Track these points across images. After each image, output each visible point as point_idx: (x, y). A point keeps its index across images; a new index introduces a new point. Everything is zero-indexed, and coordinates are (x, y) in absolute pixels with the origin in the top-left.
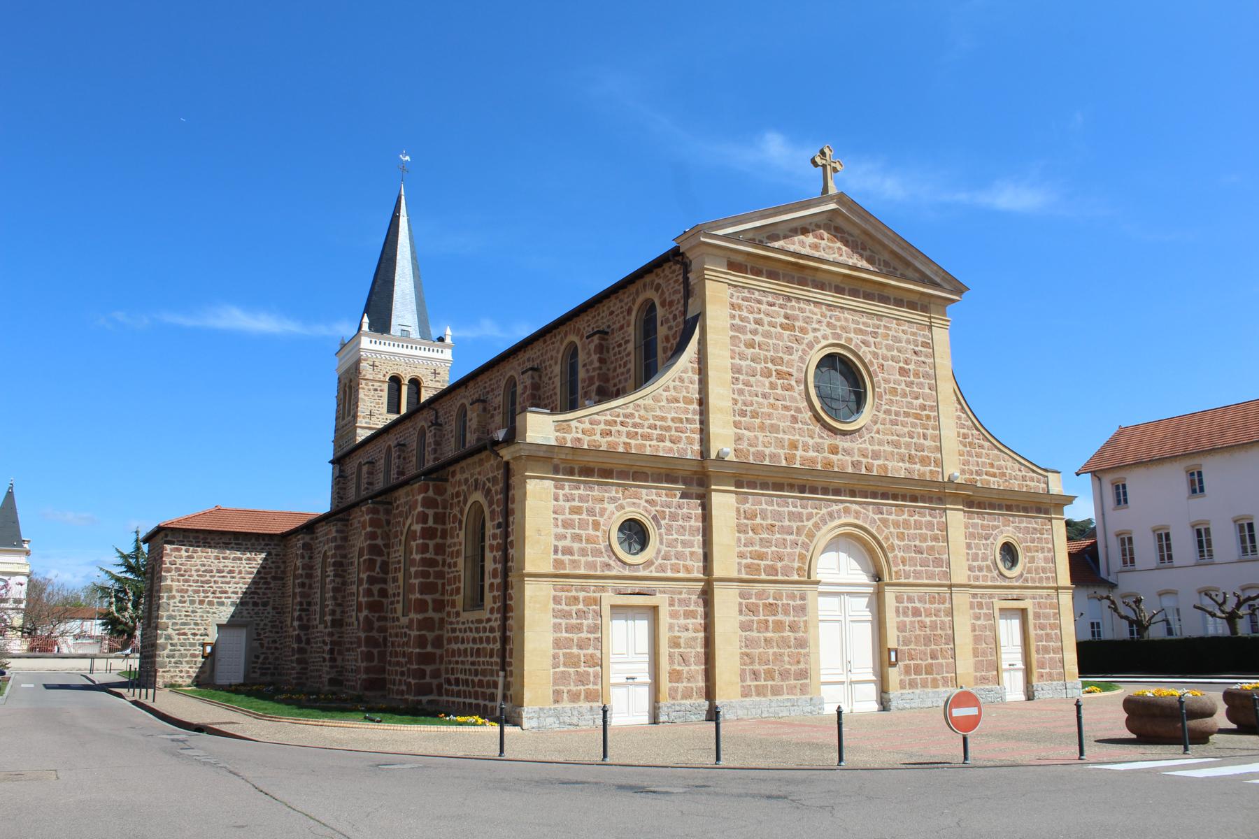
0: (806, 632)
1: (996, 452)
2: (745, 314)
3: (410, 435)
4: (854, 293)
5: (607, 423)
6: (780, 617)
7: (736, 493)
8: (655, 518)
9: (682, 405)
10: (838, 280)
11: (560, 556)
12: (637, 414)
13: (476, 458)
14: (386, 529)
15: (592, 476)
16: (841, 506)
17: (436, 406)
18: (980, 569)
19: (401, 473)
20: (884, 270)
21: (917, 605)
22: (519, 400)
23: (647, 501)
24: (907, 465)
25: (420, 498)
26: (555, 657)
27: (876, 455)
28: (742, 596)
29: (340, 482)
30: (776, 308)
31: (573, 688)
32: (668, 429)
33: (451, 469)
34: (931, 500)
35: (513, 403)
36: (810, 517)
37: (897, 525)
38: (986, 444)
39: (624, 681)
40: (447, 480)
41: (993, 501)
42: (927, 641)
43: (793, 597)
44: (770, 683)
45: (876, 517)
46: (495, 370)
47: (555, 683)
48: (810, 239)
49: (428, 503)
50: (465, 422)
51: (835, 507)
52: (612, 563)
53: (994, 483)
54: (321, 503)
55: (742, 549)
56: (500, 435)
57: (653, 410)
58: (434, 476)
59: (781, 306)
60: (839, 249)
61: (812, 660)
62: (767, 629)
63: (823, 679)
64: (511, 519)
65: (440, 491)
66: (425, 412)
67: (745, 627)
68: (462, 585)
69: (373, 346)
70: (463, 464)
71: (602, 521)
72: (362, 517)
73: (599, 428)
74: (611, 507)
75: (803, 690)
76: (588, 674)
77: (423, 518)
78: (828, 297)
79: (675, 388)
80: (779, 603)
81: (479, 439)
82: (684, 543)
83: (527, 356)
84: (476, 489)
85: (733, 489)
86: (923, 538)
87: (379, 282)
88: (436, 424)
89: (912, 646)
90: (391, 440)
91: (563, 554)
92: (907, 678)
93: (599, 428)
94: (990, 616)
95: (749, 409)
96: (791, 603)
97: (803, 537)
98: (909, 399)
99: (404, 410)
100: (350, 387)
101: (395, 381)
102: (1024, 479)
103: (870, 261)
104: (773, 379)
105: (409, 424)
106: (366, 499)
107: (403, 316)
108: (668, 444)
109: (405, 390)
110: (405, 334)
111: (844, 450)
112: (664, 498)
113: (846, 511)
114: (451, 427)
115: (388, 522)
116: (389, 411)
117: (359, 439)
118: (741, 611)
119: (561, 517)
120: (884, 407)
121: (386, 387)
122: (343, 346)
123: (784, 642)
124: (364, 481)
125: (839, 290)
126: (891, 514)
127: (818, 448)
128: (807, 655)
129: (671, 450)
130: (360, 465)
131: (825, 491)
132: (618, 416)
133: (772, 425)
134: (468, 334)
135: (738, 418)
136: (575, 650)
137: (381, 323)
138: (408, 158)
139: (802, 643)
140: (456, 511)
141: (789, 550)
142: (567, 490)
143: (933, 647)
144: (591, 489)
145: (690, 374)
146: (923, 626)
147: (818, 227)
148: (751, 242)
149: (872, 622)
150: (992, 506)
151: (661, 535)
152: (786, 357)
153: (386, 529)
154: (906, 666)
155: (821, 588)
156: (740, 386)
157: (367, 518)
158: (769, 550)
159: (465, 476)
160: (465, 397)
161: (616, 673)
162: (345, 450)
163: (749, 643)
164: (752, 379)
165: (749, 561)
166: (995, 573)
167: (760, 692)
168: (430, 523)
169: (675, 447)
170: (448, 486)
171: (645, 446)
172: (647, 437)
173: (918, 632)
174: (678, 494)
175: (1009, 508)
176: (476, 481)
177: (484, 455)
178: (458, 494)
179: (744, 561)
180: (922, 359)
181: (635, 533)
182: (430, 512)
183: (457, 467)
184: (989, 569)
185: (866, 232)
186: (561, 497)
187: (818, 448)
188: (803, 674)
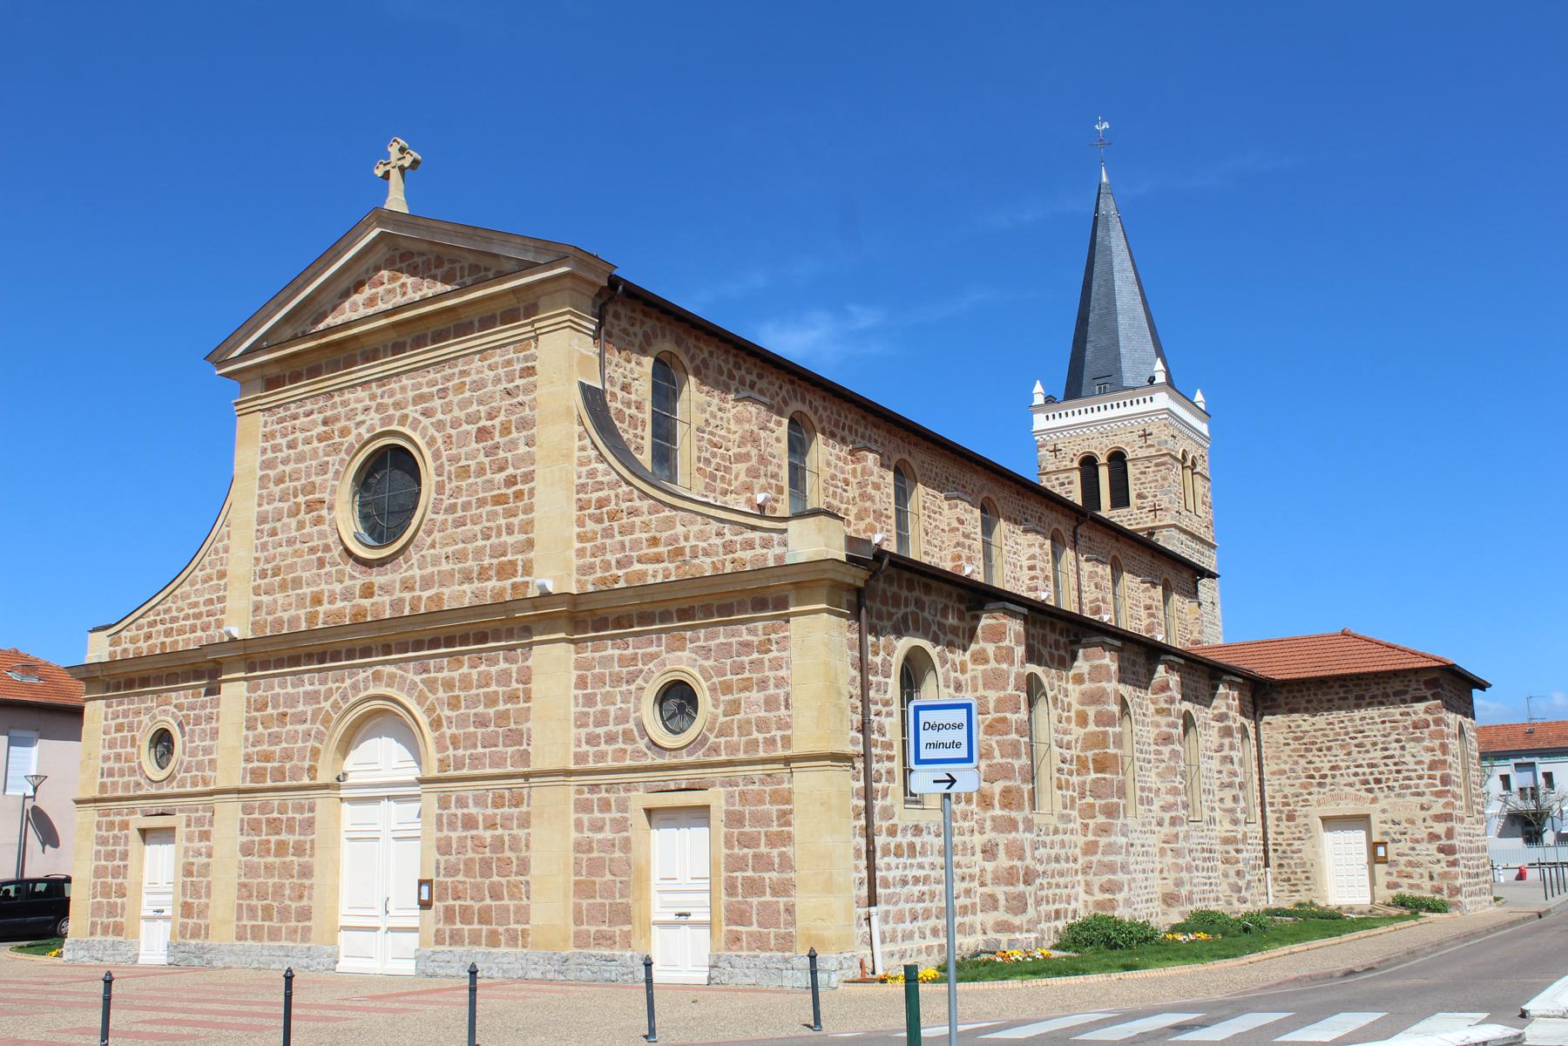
0: (312, 856)
1: (667, 513)
4: (419, 342)
6: (284, 836)
7: (245, 679)
8: (180, 725)
10: (392, 335)
16: (370, 671)
18: (611, 738)
20: (468, 280)
21: (472, 810)
24: (476, 584)
27: (427, 583)
34: (510, 634)
36: (329, 693)
38: (645, 505)
39: (673, 918)
41: (647, 608)
42: (486, 866)
43: (299, 808)
44: (267, 923)
45: (418, 679)
48: (367, 292)
51: (362, 675)
52: (142, 781)
53: (654, 573)
55: (251, 750)
60: (403, 285)
62: (268, 852)
63: (343, 922)
67: (246, 850)
69: (1052, 424)
75: (306, 934)
85: (242, 674)
86: (491, 700)
89: (460, 878)
92: (447, 928)
94: (621, 825)
96: (298, 816)
97: (318, 725)
102: (729, 548)
103: (445, 281)
109: (1104, 474)
111: (381, 588)
112: (191, 699)
113: (377, 677)
120: (447, 502)
123: (286, 870)
125: (398, 348)
126: (440, 669)
128: (311, 887)
131: (351, 654)
138: (1106, 125)
139: (306, 872)
143: (495, 878)
146: (479, 845)
147: (378, 269)
148: (270, 349)
150: (646, 618)
152: (318, 480)
154: (447, 908)
161: (660, 907)
163: (250, 870)
165: (256, 764)
166: (642, 744)
167: (257, 934)
172: (181, 631)
173: (470, 854)
174: (203, 690)
175: (685, 614)
181: (678, 698)
184: (628, 736)
187: (347, 595)
188: (305, 914)
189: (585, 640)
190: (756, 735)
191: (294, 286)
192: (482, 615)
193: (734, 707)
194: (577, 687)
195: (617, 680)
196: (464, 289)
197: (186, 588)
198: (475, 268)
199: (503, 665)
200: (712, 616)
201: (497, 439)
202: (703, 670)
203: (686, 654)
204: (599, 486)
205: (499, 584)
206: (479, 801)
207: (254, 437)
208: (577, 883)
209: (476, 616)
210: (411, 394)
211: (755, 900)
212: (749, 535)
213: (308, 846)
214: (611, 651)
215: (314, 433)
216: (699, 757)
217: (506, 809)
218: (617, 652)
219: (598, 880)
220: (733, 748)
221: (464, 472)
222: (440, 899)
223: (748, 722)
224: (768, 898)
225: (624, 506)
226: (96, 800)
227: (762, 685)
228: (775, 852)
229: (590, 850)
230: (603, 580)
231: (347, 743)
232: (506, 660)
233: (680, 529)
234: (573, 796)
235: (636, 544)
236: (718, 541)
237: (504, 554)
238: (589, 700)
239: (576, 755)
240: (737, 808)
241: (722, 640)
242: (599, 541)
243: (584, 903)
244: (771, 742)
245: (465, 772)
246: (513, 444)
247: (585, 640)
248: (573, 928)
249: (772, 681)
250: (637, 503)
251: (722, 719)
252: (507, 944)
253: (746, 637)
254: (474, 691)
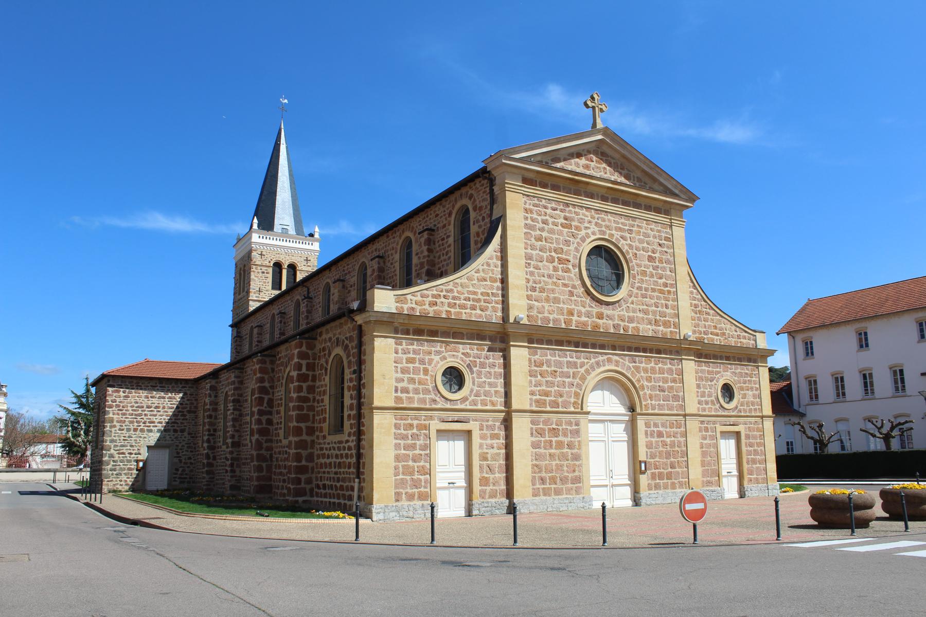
0: (579, 449)
1: (718, 317)
2: (535, 216)
3: (288, 306)
4: (615, 201)
5: (434, 296)
6: (560, 438)
7: (528, 347)
8: (469, 366)
9: (488, 283)
10: (603, 191)
11: (399, 394)
12: (455, 290)
13: (337, 323)
14: (272, 375)
15: (423, 335)
16: (605, 357)
17: (308, 284)
18: (707, 403)
19: (282, 334)
20: (637, 185)
21: (661, 429)
22: (369, 279)
23: (463, 354)
24: (654, 327)
25: (296, 352)
26: (396, 468)
27: (631, 320)
28: (533, 423)
29: (237, 340)
30: (558, 212)
31: (410, 491)
32: (479, 300)
33: (319, 330)
34: (671, 353)
35: (365, 282)
37: (646, 370)
38: (712, 312)
39: (447, 485)
40: (316, 339)
42: (668, 455)
43: (570, 423)
44: (553, 486)
45: (631, 365)
46: (351, 258)
47: (396, 487)
48: (583, 161)
49: (302, 356)
50: (329, 296)
51: (601, 358)
52: (437, 399)
53: (717, 340)
54: (224, 357)
55: (533, 388)
56: (355, 305)
57: (467, 287)
58: (307, 336)
59: (562, 211)
60: (605, 168)
61: (584, 469)
62: (551, 447)
63: (592, 483)
64: (363, 367)
65: (311, 347)
66: (300, 289)
67: (535, 445)
68: (327, 416)
69: (261, 241)
70: (328, 327)
71: (430, 368)
72: (254, 366)
73: (427, 300)
74: (436, 358)
76: (421, 480)
77: (299, 367)
78: (596, 204)
79: (483, 270)
80: (560, 428)
81: (339, 309)
82: (490, 384)
83: (374, 247)
84: (337, 345)
85: (526, 344)
86: (665, 381)
87: (265, 192)
88: (308, 297)
89: (657, 459)
90: (275, 310)
91: (402, 392)
92: (653, 483)
93: (427, 300)
94: (714, 437)
95: (538, 286)
96: (569, 428)
98: (655, 279)
99: (284, 287)
100: (244, 271)
101: (278, 266)
102: (739, 337)
103: (627, 177)
104: (556, 264)
105: (288, 297)
106: (257, 353)
107: (283, 218)
108: (478, 312)
109: (284, 272)
110: (285, 232)
111: (607, 316)
112: (476, 351)
113: (609, 360)
114: (319, 300)
115: (273, 370)
116: (273, 288)
117: (251, 309)
118: (532, 434)
119: (399, 366)
120: (637, 285)
121: (270, 270)
122: (239, 240)
123: (564, 457)
124: (255, 340)
125: (604, 199)
126: (641, 363)
127: (588, 315)
128: (580, 466)
129: (481, 316)
130: (252, 328)
131: (594, 346)
132: (442, 291)
133: (555, 298)
134: (331, 232)
135: (530, 293)
136: (411, 463)
137: (267, 224)
138: (286, 101)
139: (577, 457)
140: (323, 361)
141: (567, 389)
142: (404, 346)
144: (422, 345)
145: (495, 260)
146: (665, 444)
147: (589, 152)
148: (540, 163)
149: (628, 442)
150: (715, 357)
151: (473, 378)
152: (565, 248)
153: (272, 375)
155: (590, 417)
156: (532, 269)
157: (257, 367)
158: (553, 390)
159: (330, 335)
160: (329, 278)
161: (440, 480)
162: (241, 317)
163: (538, 457)
164: (540, 264)
165: (538, 397)
166: (717, 406)
167: (546, 493)
168: (304, 370)
169: (483, 314)
170: (317, 343)
171: (461, 313)
172: (463, 307)
173: (661, 449)
174: (486, 348)
175: (728, 358)
176: (338, 339)
177: (343, 320)
178: (324, 349)
179: (534, 397)
180: (665, 249)
181: (454, 377)
182: (304, 362)
183: (323, 329)
185: (624, 157)
186: (400, 351)
187: (588, 315)
188: (578, 480)
191: (559, 141)
196: (634, 187)
197: (464, 280)
213: (577, 443)
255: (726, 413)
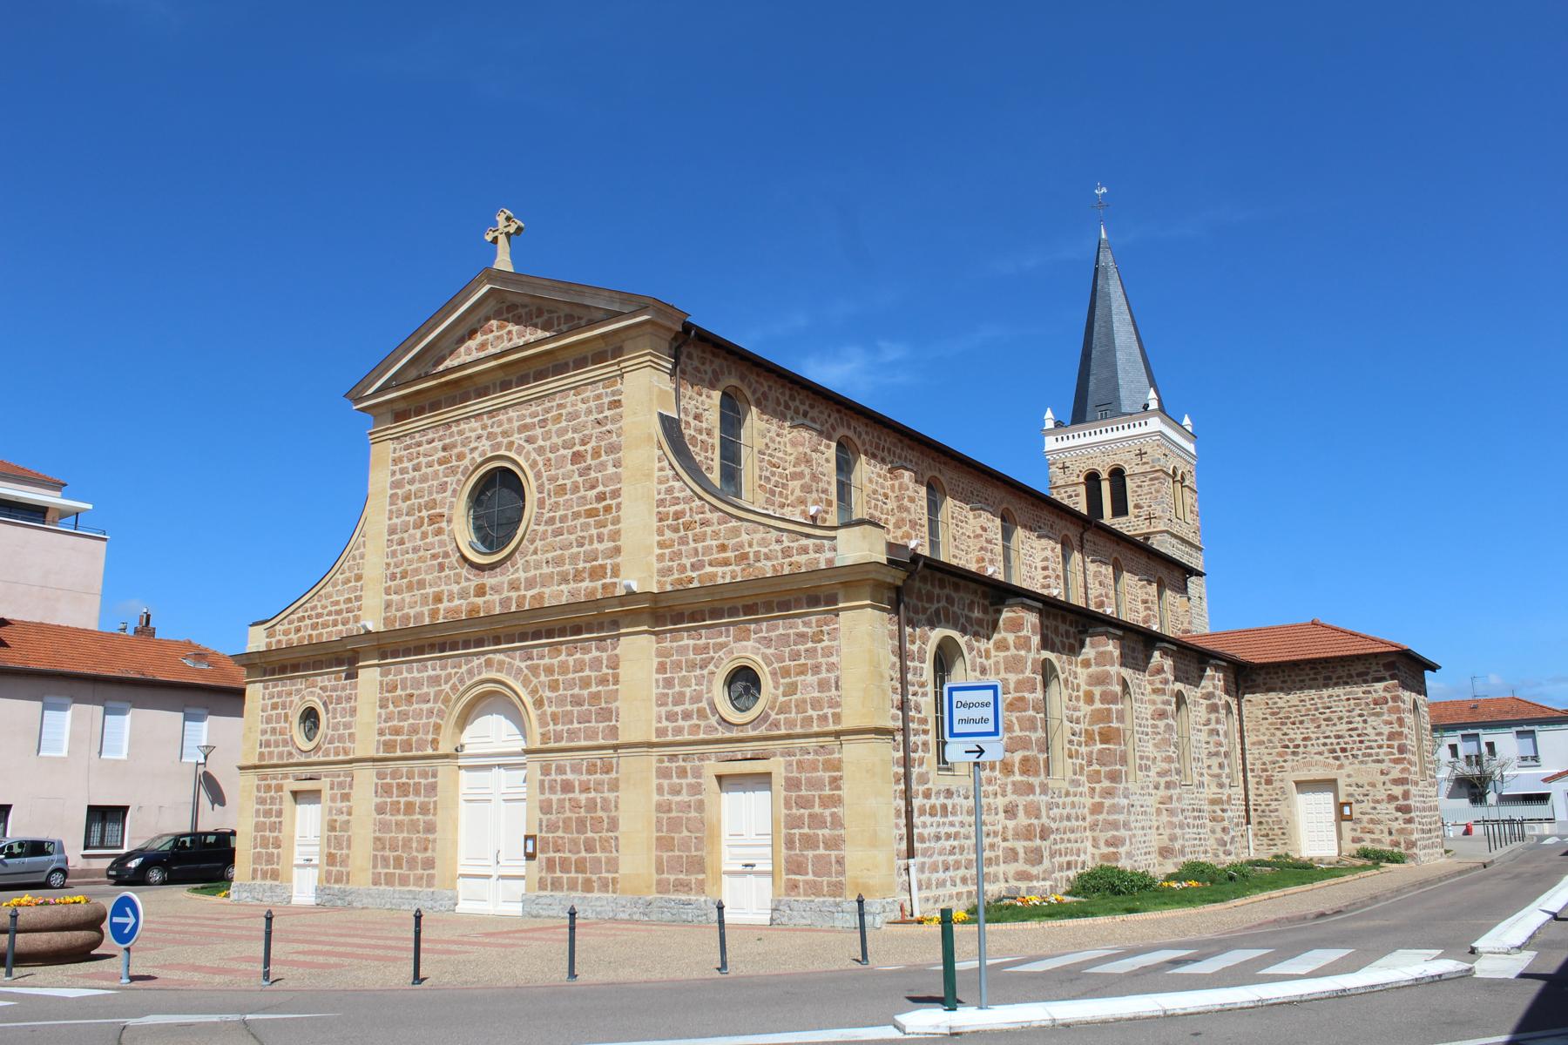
1: (734, 523)
4: (523, 380)
6: (411, 798)
8: (325, 704)
10: (500, 375)
16: (483, 659)
18: (687, 716)
20: (564, 328)
21: (570, 776)
24: (572, 585)
27: (530, 584)
34: (601, 628)
36: (449, 677)
38: (715, 516)
39: (740, 868)
41: (717, 605)
42: (581, 824)
43: (424, 775)
45: (523, 665)
48: (479, 338)
51: (476, 662)
53: (723, 575)
55: (383, 725)
60: (510, 332)
62: (398, 811)
63: (461, 870)
67: (380, 810)
69: (1061, 445)
86: (586, 683)
89: (560, 834)
92: (549, 877)
94: (696, 789)
102: (786, 553)
103: (544, 329)
109: (1106, 487)
113: (489, 664)
123: (414, 826)
125: (505, 386)
126: (542, 657)
127: (463, 594)
128: (434, 841)
131: (466, 645)
138: (1104, 190)
139: (430, 828)
143: (590, 834)
146: (576, 806)
147: (488, 319)
148: (398, 387)
150: (716, 613)
152: (438, 497)
154: (548, 859)
161: (729, 859)
163: (384, 826)
165: (388, 737)
166: (713, 720)
167: (389, 880)
172: (325, 625)
173: (568, 814)
175: (749, 609)
181: (744, 681)
184: (701, 714)
187: (463, 594)
188: (429, 864)
189: (664, 632)
190: (810, 712)
191: (418, 335)
192: (577, 611)
193: (791, 689)
194: (658, 671)
195: (692, 666)
196: (561, 335)
197: (329, 589)
198: (569, 318)
199: (595, 653)
200: (772, 611)
201: (589, 461)
202: (765, 657)
203: (750, 643)
204: (676, 501)
205: (591, 585)
206: (576, 769)
207: (385, 462)
208: (658, 839)
209: (572, 612)
210: (516, 424)
211: (810, 853)
212: (804, 541)
214: (687, 641)
215: (435, 457)
216: (762, 731)
217: (598, 776)
218: (692, 642)
219: (676, 836)
220: (790, 723)
221: (561, 490)
222: (542, 851)
223: (804, 701)
224: (821, 851)
225: (697, 517)
226: (256, 767)
227: (816, 669)
228: (827, 812)
229: (670, 810)
230: (680, 581)
231: (464, 720)
232: (597, 649)
233: (745, 537)
234: (655, 765)
235: (707, 550)
236: (778, 547)
237: (595, 559)
238: (669, 683)
239: (657, 729)
240: (795, 774)
241: (781, 631)
242: (676, 548)
243: (665, 855)
244: (824, 718)
245: (563, 744)
246: (603, 466)
247: (664, 632)
248: (655, 877)
249: (824, 668)
250: (708, 515)
251: (781, 699)
252: (600, 890)
253: (802, 629)
254: (571, 676)
255: (735, 734)
